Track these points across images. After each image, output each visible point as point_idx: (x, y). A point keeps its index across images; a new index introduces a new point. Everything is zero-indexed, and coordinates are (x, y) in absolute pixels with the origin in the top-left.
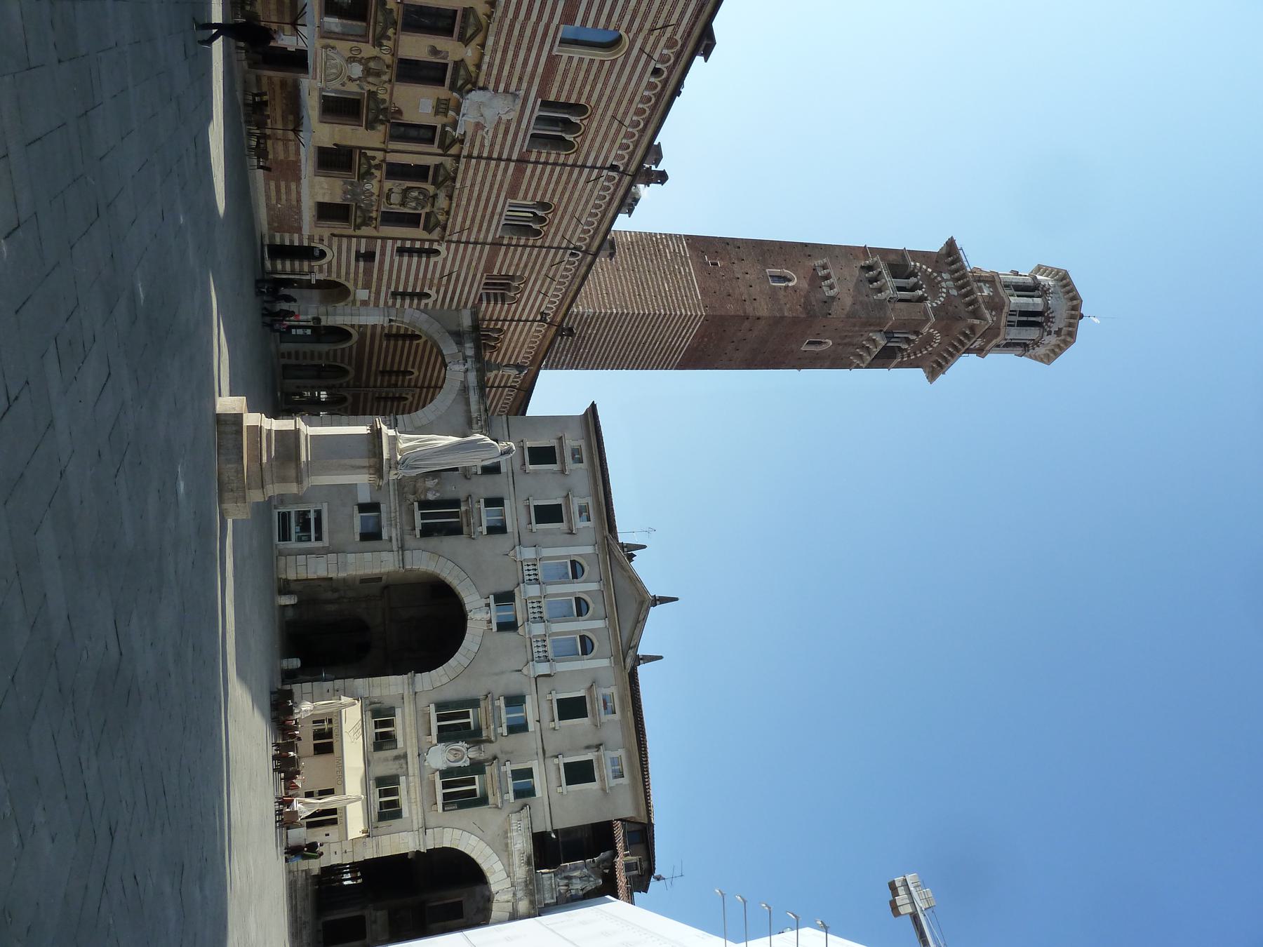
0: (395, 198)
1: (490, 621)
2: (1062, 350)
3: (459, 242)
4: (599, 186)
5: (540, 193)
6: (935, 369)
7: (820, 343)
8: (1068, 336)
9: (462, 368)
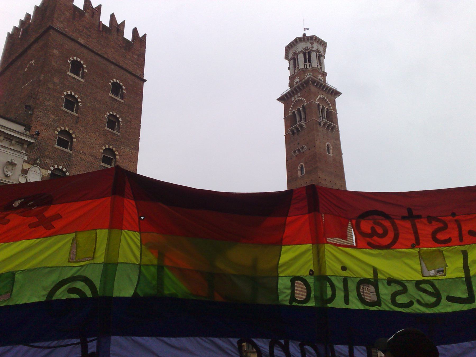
2: (319, 39)
7: (328, 147)
8: (313, 39)
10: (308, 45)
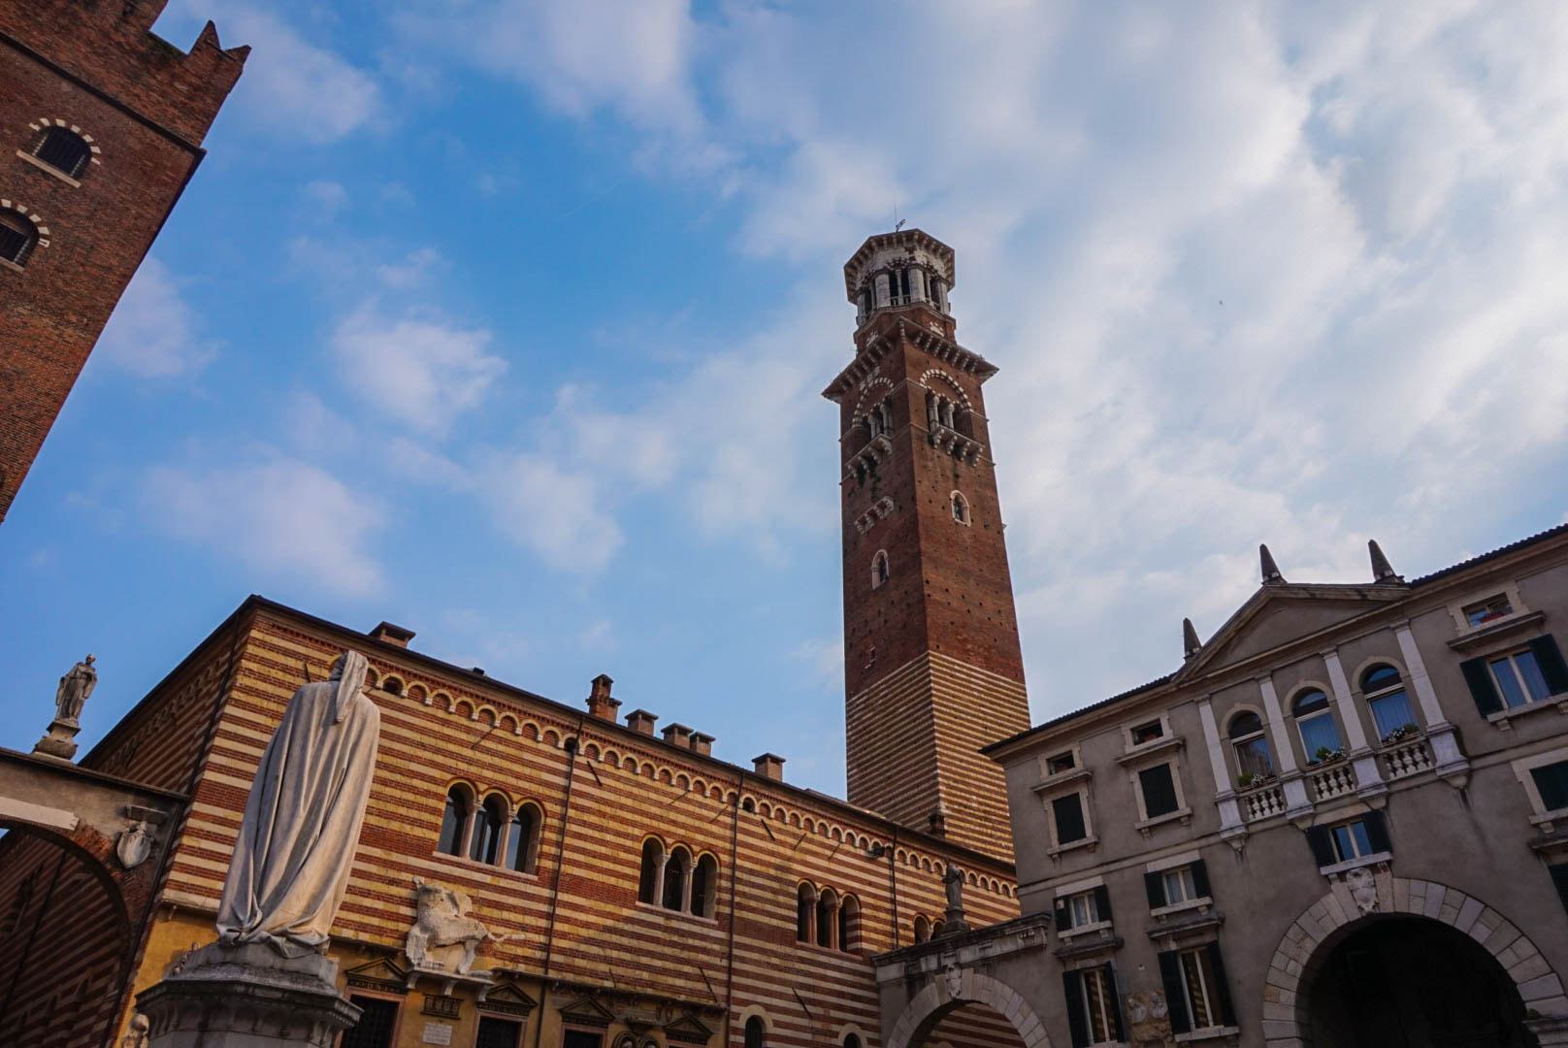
1: (1373, 868)
2: (931, 240)
3: (729, 985)
4: (609, 768)
6: (983, 369)
7: (958, 503)
8: (913, 239)
9: (956, 973)
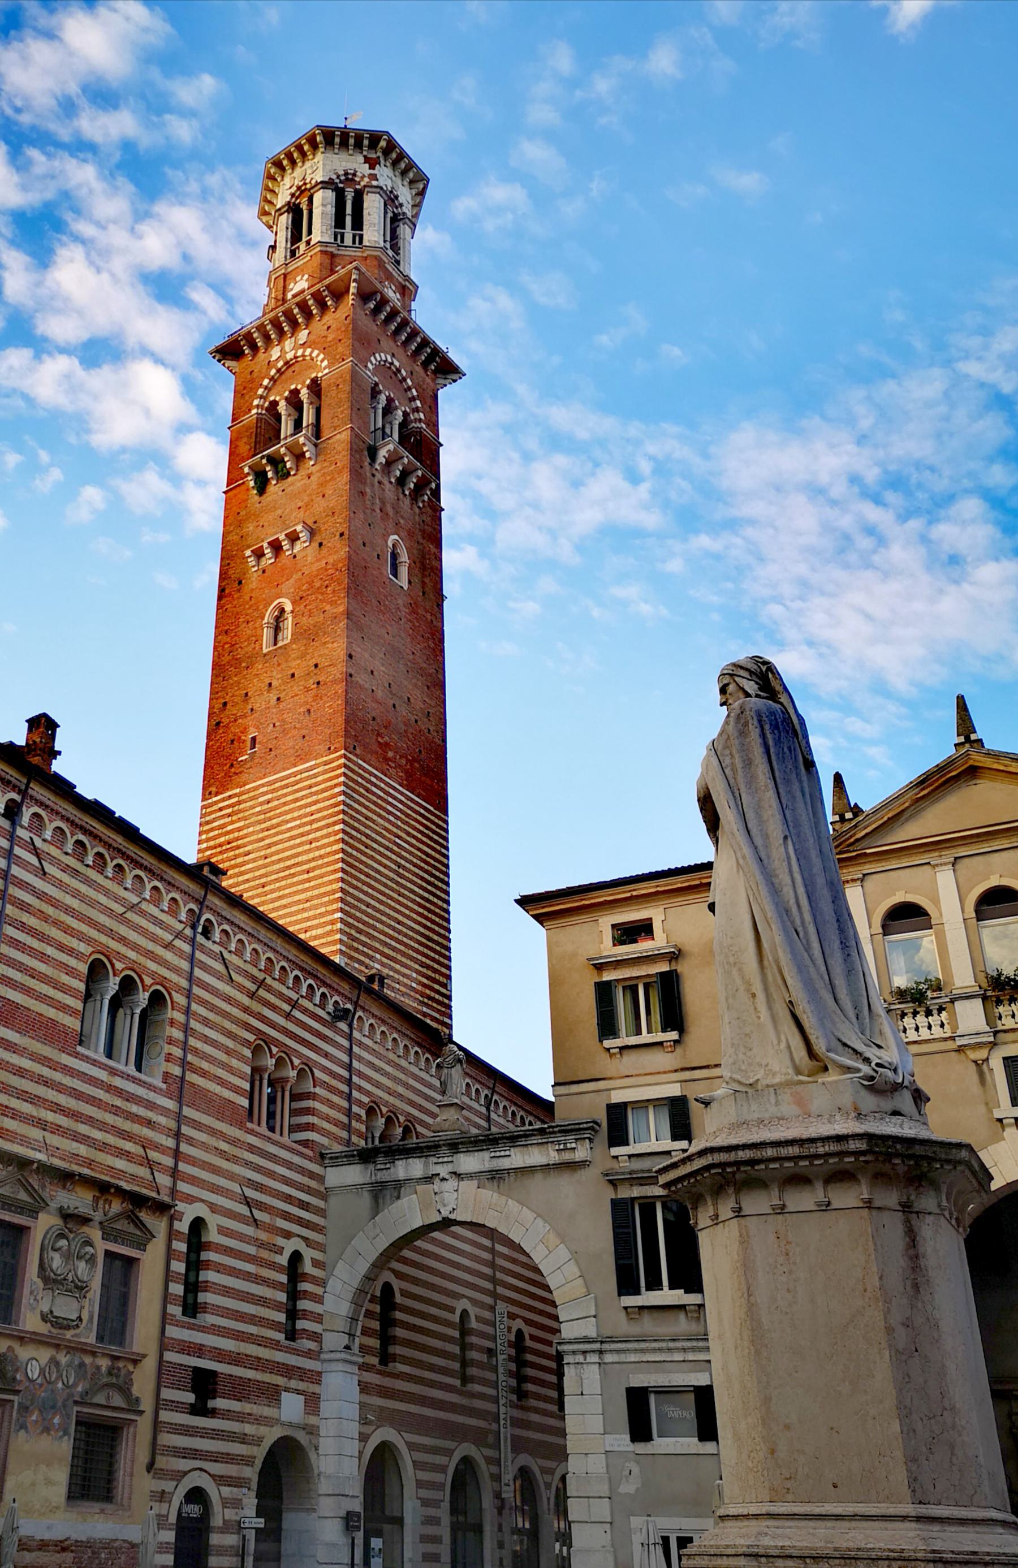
0: (66, 1308)
3: (175, 1173)
5: (65, 979)
7: (394, 556)
8: (378, 146)
10: (355, 163)
